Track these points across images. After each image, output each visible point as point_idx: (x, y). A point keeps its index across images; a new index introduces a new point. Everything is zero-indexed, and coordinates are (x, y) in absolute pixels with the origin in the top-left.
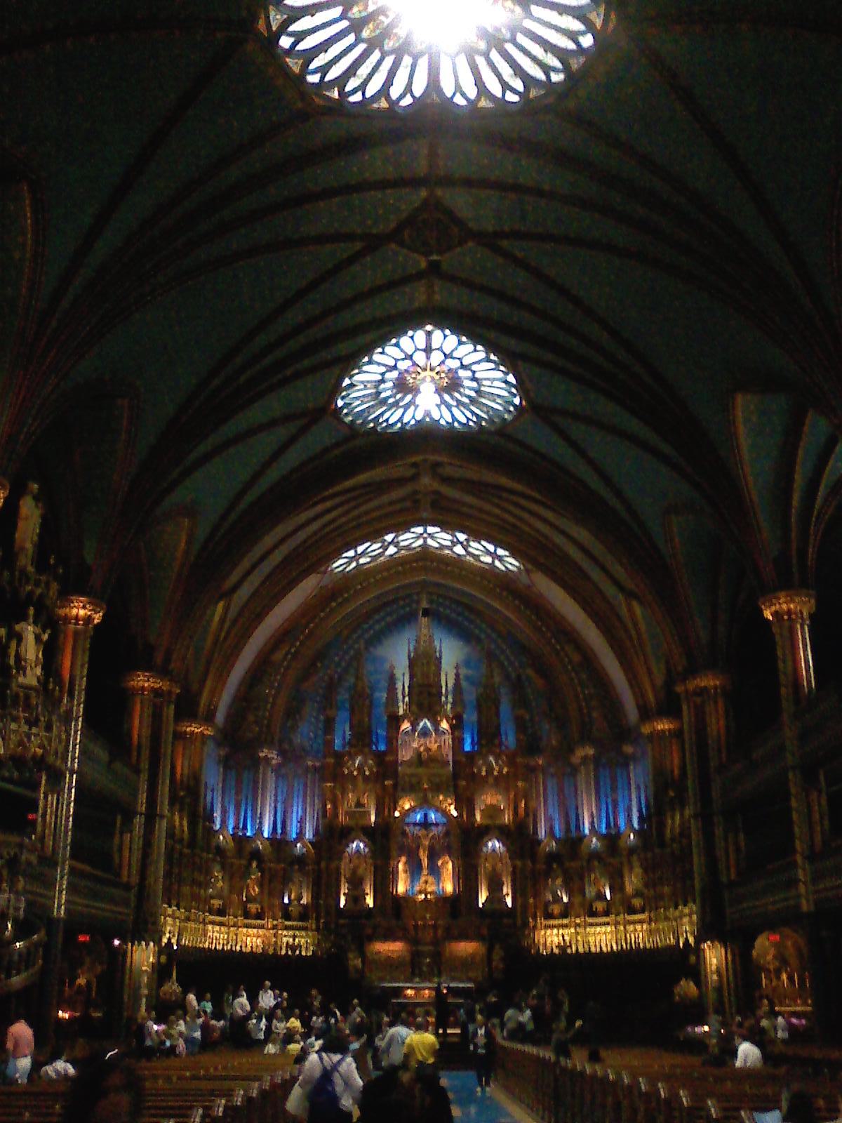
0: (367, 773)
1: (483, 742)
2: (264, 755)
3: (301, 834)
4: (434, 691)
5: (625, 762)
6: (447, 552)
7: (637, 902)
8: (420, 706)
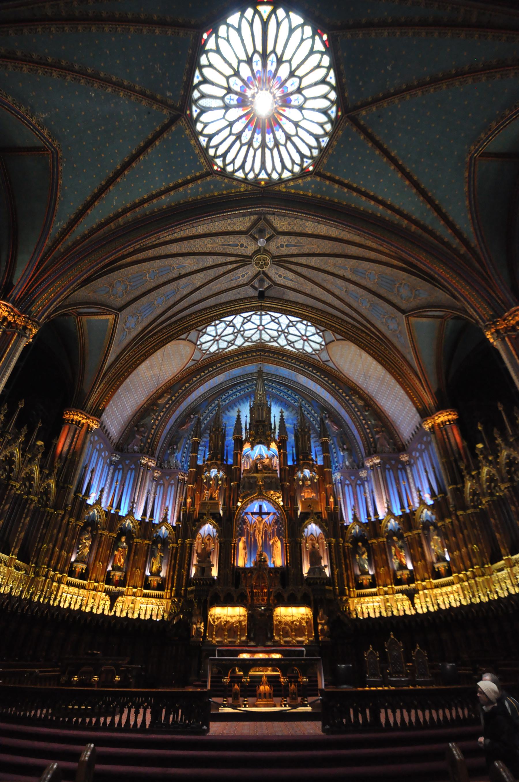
0: (220, 483)
1: (301, 457)
2: (145, 462)
3: (165, 520)
4: (267, 423)
5: (404, 466)
6: (274, 344)
7: (441, 566)
8: (257, 433)
